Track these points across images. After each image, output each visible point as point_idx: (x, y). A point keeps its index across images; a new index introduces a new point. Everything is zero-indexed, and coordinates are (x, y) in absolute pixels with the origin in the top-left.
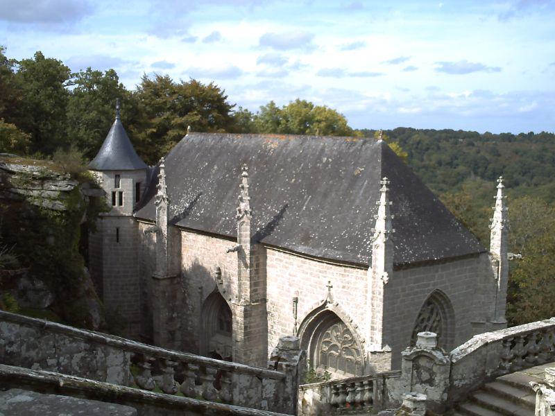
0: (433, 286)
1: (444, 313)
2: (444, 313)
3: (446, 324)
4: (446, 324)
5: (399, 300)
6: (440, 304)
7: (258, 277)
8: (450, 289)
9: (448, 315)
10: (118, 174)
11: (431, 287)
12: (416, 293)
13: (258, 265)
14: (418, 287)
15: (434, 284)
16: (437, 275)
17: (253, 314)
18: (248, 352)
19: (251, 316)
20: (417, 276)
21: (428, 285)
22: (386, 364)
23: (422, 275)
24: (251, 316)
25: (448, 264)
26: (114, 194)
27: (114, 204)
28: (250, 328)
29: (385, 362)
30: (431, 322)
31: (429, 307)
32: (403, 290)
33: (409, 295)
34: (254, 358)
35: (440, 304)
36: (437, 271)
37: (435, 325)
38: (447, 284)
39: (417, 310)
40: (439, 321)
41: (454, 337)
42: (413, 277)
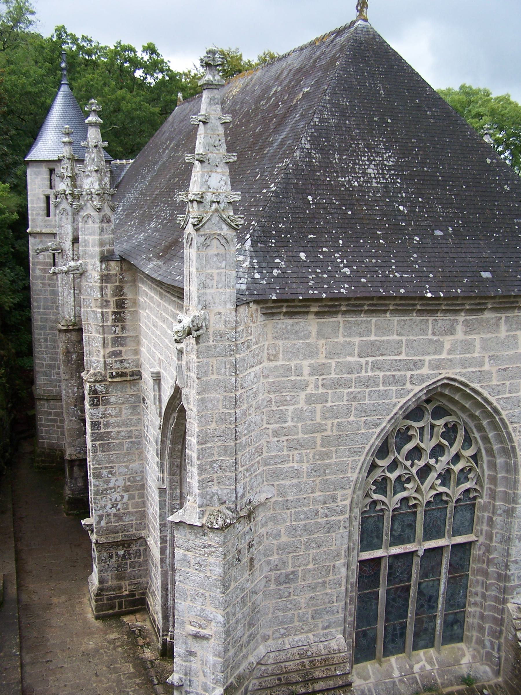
0: (431, 367)
1: (486, 439)
2: (486, 439)
3: (493, 465)
4: (493, 465)
5: (302, 395)
6: (472, 416)
7: (123, 328)
8: (494, 382)
9: (496, 447)
10: (52, 166)
11: (425, 371)
12: (366, 383)
13: (120, 304)
14: (376, 366)
15: (438, 365)
16: (448, 341)
17: (113, 399)
18: (105, 472)
19: (107, 402)
20: (373, 338)
21: (417, 365)
22: (211, 560)
23: (395, 337)
24: (107, 402)
25: (488, 315)
26: (48, 198)
27: (48, 215)
28: (107, 425)
29: (210, 554)
30: (444, 459)
31: (441, 422)
32: (316, 371)
33: (337, 384)
34: (121, 482)
35: (472, 416)
36: (451, 331)
37: (457, 468)
38: (486, 367)
39: (377, 425)
40: (475, 457)
41: (515, 502)
42: (357, 340)
